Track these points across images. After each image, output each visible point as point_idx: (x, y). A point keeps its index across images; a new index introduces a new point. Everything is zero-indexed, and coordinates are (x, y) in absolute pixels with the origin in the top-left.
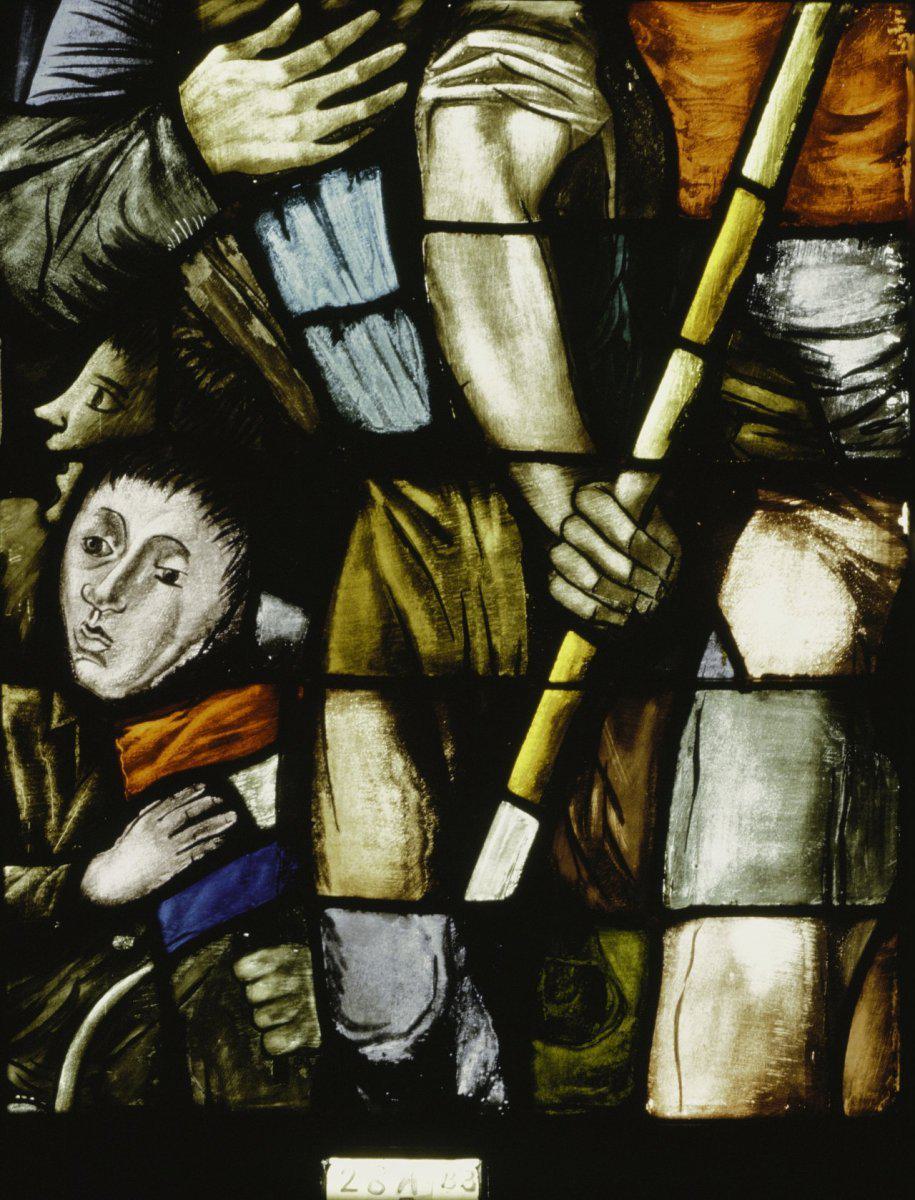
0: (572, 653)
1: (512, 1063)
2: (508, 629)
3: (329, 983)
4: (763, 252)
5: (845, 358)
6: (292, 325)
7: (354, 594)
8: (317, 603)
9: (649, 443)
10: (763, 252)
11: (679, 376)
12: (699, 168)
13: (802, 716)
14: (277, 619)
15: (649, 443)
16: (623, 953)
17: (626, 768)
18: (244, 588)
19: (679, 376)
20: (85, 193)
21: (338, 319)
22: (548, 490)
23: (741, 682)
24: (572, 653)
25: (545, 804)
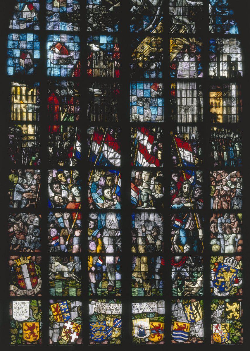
0: (69, 235)
1: (67, 251)
2: (67, 235)
3: (61, 248)
4: (76, 221)
5: (79, 225)
6: (59, 223)
7: (61, 233)
8: (60, 233)
9: (72, 227)
10: (76, 221)
11: (73, 225)
12: (74, 218)
13: (78, 238)
14: (58, 234)
15: (72, 227)
16: (71, 246)
17: (71, 240)
18: (57, 233)
19: (73, 225)
20: (51, 218)
21: (61, 223)
22: (68, 229)
23: (76, 236)
24: (69, 235)
25: (68, 241)
